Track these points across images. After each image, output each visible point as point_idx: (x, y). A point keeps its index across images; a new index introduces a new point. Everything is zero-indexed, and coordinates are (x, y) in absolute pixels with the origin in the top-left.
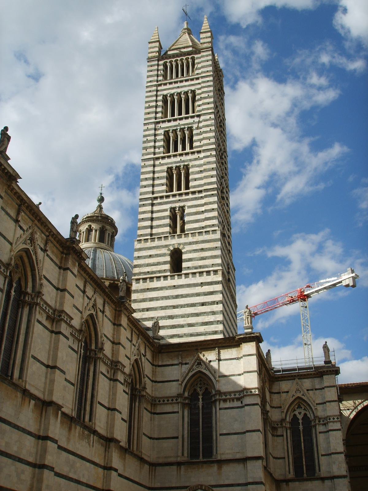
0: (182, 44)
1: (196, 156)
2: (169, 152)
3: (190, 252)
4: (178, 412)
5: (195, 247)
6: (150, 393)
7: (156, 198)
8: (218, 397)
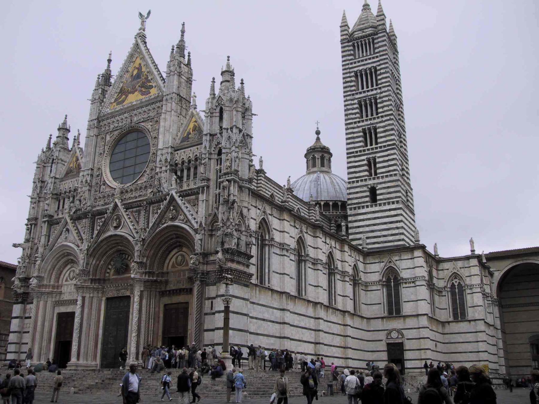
0: (364, 24)
1: (380, 120)
2: (363, 118)
3: (381, 189)
4: (380, 290)
5: (384, 185)
6: (364, 280)
7: (357, 152)
8: (401, 281)
